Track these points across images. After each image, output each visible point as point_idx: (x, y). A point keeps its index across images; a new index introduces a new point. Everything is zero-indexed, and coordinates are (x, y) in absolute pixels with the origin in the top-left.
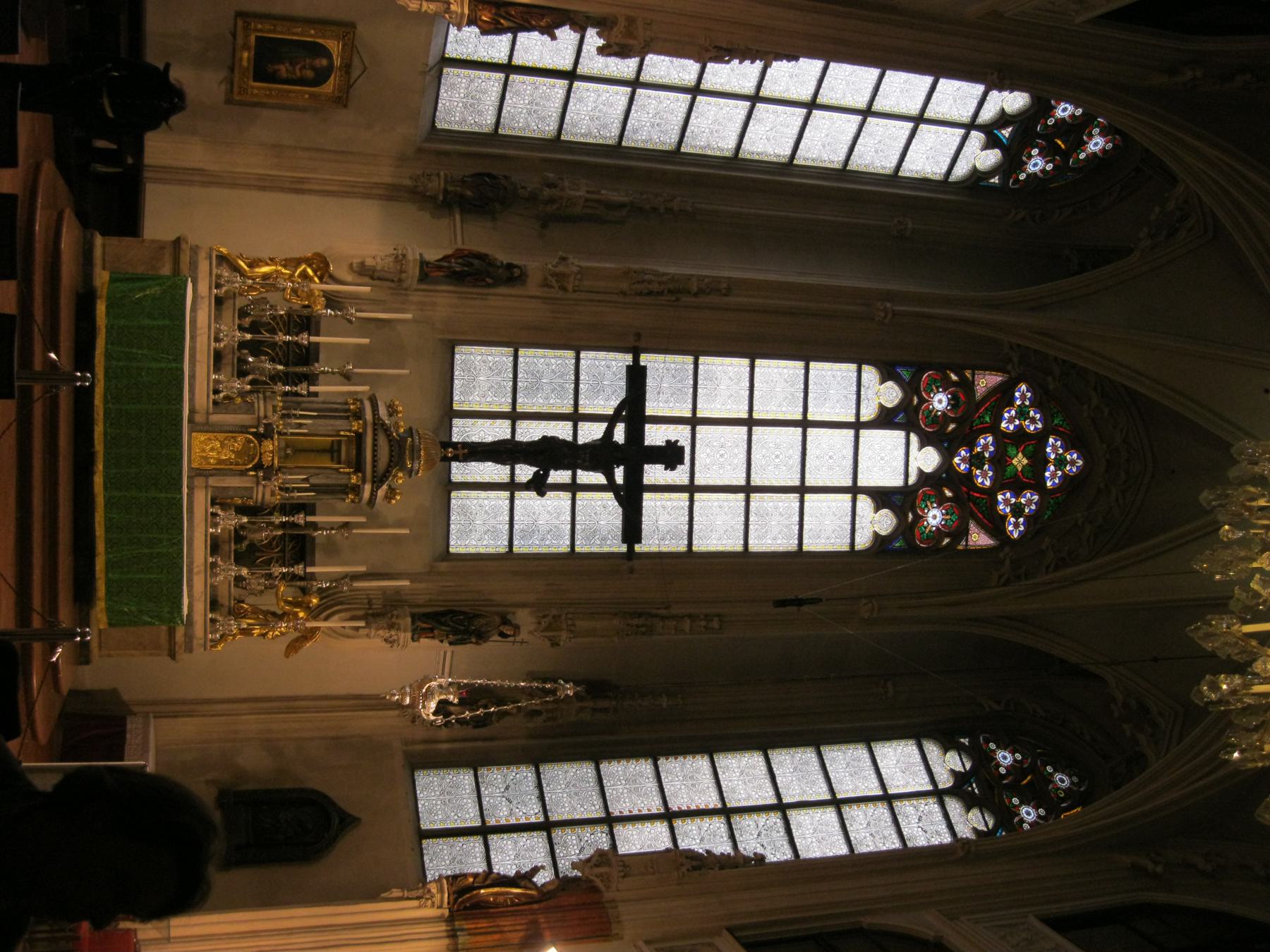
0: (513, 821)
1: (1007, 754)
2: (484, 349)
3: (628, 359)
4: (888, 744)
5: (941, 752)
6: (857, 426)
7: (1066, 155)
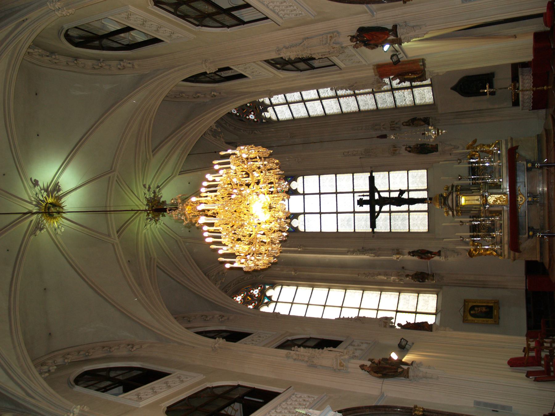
0: (403, 91)
1: (251, 118)
2: (419, 231)
3: (375, 230)
5: (271, 117)
6: (304, 213)
7: (247, 295)
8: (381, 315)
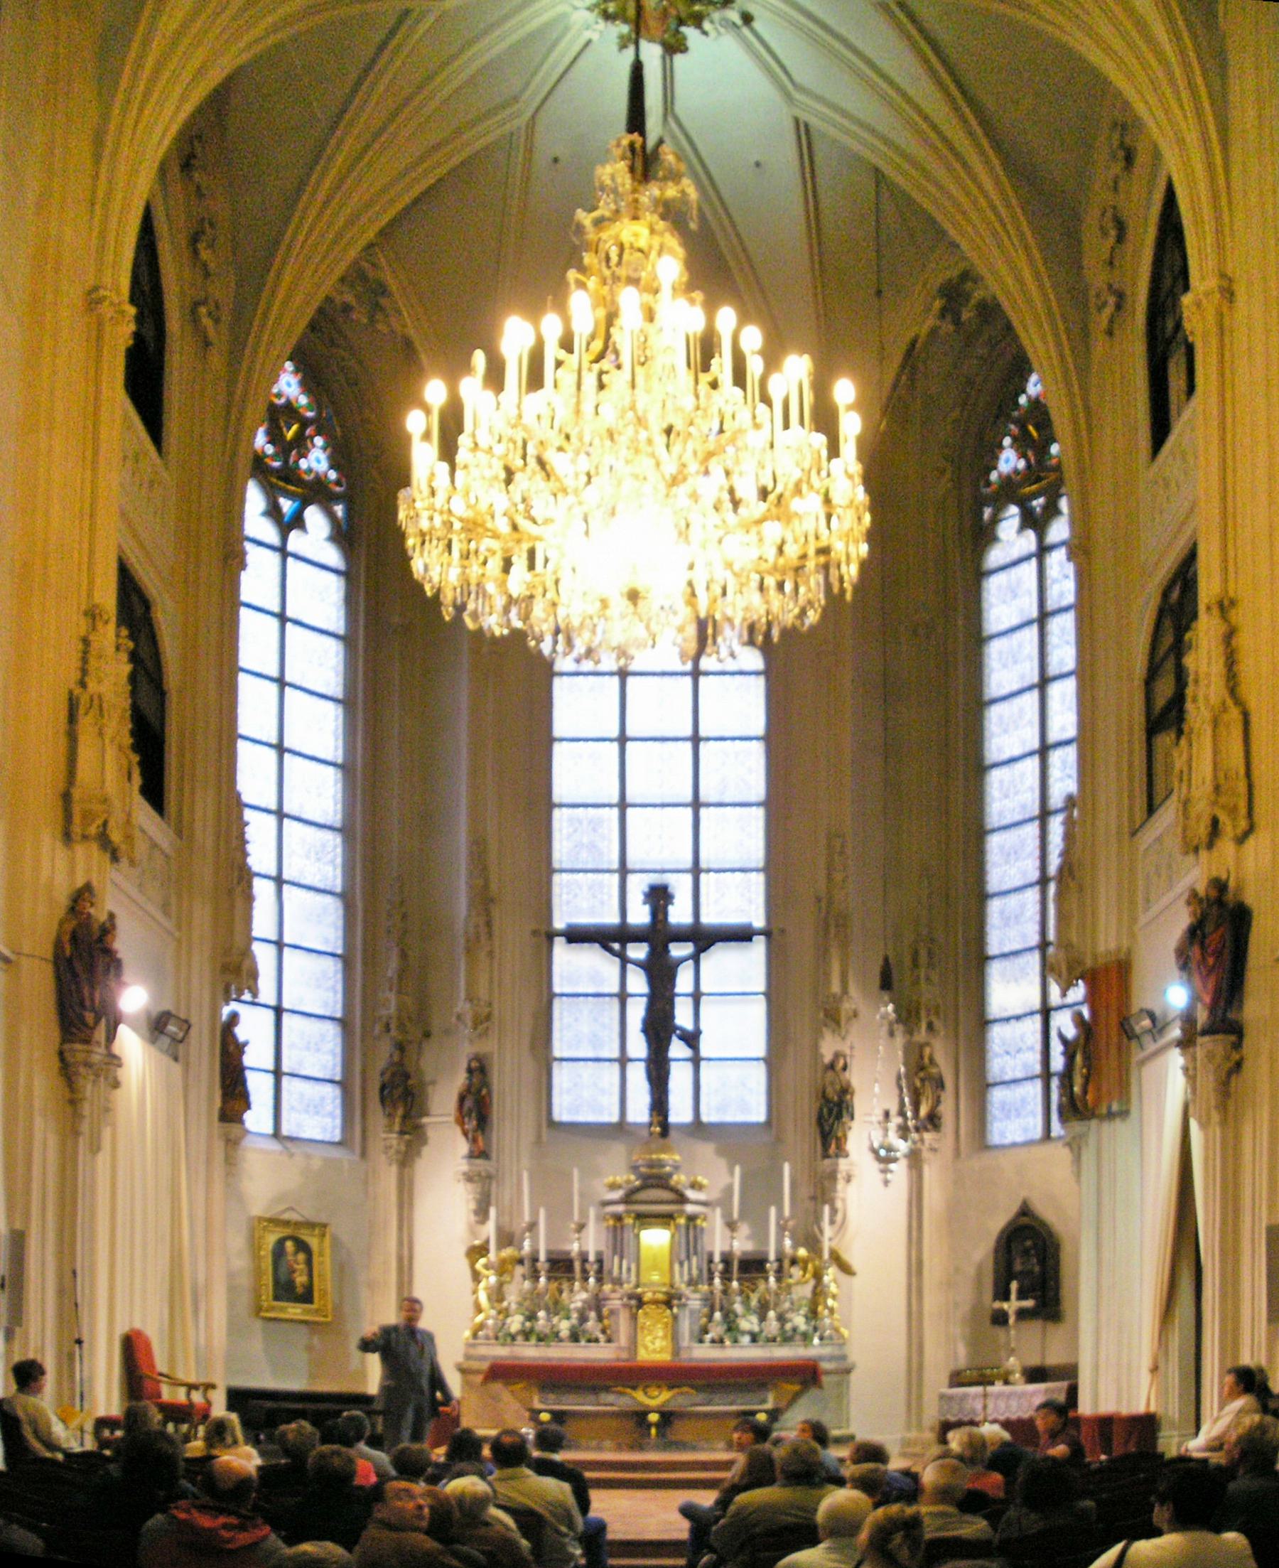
4: (985, 615)
8: (264, 956)
